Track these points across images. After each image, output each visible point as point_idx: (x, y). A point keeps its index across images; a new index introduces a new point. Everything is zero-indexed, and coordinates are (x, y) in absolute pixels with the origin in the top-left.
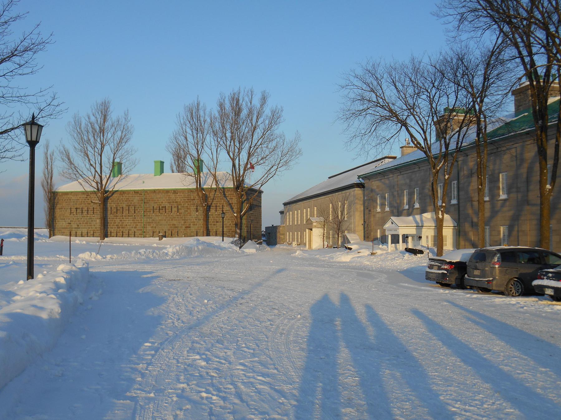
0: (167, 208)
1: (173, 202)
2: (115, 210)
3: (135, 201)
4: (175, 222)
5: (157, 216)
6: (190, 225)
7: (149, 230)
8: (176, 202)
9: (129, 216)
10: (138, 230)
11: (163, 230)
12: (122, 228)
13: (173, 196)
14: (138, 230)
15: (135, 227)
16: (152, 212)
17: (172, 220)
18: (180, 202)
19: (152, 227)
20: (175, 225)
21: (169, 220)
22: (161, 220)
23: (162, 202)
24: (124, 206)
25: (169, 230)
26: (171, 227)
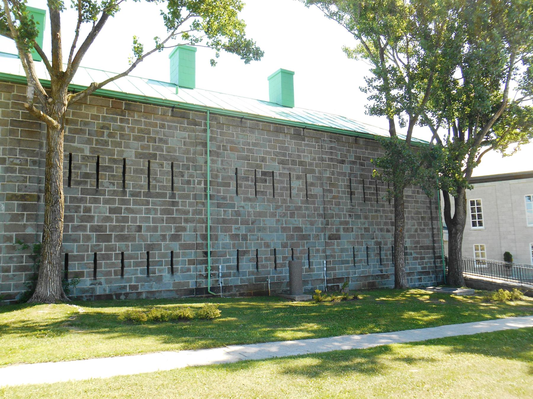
0: (277, 177)
1: (294, 163)
2: (90, 169)
3: (172, 142)
4: (298, 222)
5: (247, 199)
6: (338, 230)
7: (225, 246)
8: (301, 163)
9: (148, 194)
10: (185, 247)
11: (267, 245)
12: (122, 238)
13: (291, 144)
14: (185, 247)
15: (175, 238)
16: (233, 188)
17: (292, 215)
18: (311, 164)
19: (235, 237)
20: (298, 229)
21: (285, 215)
22: (261, 214)
23: (263, 160)
24: (130, 154)
25: (284, 246)
26: (291, 237)
